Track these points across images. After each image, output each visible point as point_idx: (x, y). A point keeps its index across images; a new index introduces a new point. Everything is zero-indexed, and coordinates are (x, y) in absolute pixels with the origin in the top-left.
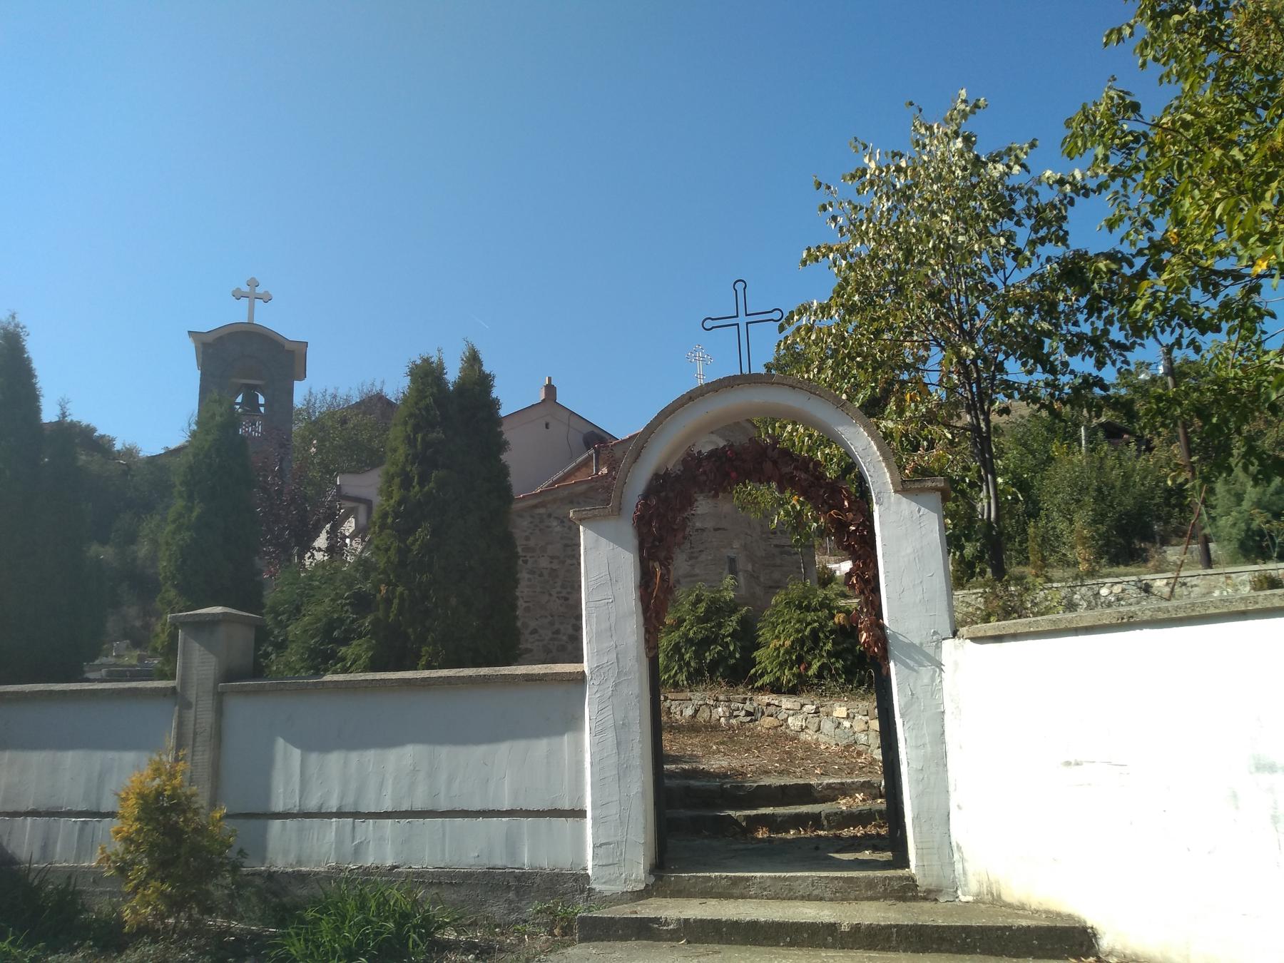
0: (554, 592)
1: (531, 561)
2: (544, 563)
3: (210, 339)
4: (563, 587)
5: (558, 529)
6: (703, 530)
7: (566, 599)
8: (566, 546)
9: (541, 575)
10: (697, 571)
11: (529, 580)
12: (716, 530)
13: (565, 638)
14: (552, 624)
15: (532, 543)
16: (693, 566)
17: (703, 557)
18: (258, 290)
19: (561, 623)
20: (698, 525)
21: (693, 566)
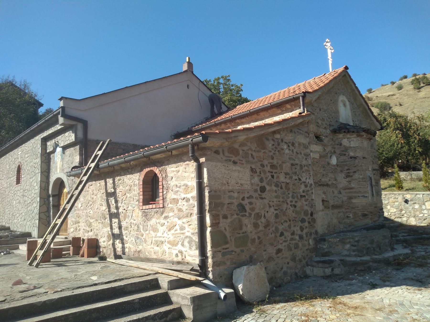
0: (288, 201)
1: (275, 176)
2: (282, 178)
4: (293, 197)
5: (287, 151)
6: (355, 158)
8: (292, 165)
9: (281, 188)
10: (353, 185)
11: (276, 192)
12: (364, 158)
13: (297, 238)
14: (290, 227)
15: (275, 162)
16: (349, 182)
17: (356, 176)
19: (295, 226)
20: (352, 154)
21: (349, 182)
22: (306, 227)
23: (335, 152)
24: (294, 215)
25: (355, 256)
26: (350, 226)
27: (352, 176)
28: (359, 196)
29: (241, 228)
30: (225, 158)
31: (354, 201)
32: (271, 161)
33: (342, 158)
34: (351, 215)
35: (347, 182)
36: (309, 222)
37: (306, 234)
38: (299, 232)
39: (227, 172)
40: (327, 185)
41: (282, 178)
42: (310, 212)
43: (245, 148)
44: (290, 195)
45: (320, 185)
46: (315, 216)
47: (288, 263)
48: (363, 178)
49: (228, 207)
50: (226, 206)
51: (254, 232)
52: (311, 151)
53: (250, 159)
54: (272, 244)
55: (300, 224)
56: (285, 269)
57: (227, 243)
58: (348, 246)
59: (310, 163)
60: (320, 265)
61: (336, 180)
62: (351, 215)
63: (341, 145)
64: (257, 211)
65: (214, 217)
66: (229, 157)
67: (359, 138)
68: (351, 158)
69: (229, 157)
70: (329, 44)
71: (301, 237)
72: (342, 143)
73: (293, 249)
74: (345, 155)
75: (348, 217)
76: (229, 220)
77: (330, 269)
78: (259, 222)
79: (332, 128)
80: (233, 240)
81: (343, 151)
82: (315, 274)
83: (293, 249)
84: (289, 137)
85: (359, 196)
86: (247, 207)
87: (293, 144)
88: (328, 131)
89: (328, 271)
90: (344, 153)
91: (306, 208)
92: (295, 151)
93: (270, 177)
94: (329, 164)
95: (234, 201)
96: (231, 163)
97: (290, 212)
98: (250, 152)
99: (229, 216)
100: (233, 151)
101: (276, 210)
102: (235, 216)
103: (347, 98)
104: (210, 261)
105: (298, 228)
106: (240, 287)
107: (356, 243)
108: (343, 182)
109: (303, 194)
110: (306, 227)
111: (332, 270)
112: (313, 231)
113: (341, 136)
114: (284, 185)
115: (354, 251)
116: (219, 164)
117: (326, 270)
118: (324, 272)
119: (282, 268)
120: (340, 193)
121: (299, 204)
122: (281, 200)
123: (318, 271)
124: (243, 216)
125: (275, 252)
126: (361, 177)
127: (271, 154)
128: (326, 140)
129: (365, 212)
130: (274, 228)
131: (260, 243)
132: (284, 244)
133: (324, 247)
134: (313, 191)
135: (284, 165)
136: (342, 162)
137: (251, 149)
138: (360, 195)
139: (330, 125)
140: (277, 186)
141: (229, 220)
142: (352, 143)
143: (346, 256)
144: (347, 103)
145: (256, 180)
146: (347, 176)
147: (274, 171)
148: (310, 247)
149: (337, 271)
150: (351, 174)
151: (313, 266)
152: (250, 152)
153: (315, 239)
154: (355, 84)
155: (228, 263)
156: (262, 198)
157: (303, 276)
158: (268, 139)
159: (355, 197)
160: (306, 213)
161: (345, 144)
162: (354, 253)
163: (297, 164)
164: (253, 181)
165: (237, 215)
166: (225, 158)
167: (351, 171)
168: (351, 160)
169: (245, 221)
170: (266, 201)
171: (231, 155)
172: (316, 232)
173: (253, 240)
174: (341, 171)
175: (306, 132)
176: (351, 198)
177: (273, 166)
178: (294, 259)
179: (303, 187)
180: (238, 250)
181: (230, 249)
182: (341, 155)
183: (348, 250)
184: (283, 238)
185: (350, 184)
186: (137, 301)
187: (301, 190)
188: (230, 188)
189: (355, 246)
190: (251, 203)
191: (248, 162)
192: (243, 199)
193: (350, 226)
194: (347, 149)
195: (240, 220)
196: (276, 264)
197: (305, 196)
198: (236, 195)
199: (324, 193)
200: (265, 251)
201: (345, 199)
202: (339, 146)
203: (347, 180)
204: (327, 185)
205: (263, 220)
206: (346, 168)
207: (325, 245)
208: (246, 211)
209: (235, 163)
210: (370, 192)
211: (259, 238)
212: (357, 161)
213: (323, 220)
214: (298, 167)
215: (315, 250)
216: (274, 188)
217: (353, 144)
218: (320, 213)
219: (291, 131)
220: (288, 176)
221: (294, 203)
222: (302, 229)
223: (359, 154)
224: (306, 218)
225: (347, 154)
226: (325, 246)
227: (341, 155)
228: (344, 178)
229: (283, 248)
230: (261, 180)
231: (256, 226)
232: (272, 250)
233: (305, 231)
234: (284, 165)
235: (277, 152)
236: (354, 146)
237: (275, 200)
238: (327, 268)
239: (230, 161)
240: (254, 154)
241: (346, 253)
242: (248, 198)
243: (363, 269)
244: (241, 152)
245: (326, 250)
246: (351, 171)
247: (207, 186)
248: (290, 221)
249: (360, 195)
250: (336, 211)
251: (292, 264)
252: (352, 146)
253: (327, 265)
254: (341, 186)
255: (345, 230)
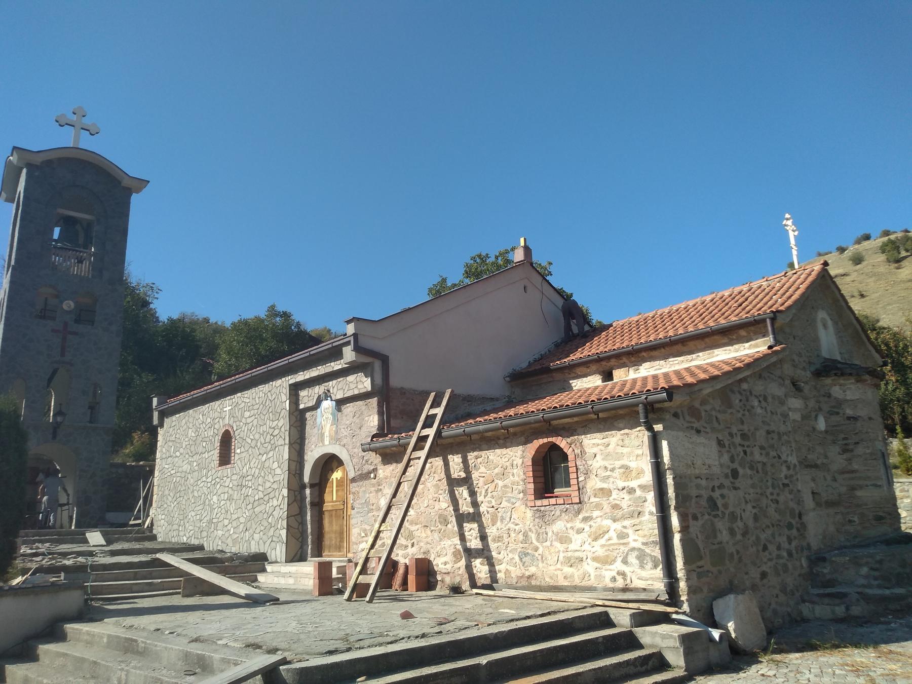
3: (38, 160)
5: (759, 411)
6: (855, 419)
7: (777, 502)
8: (768, 432)
9: (758, 472)
10: (855, 466)
13: (785, 554)
14: (773, 535)
15: (745, 428)
16: (849, 460)
17: (860, 450)
18: (86, 121)
19: (780, 535)
20: (849, 412)
21: (849, 460)
22: (795, 538)
23: (820, 409)
24: (778, 517)
25: (879, 587)
26: (856, 537)
27: (852, 451)
28: (867, 486)
29: (715, 537)
30: (686, 425)
31: (859, 493)
32: (741, 427)
33: (835, 419)
34: (856, 519)
35: (846, 460)
36: (798, 530)
37: (796, 548)
38: (786, 545)
39: (690, 446)
40: (816, 466)
41: (757, 457)
42: (797, 512)
43: (708, 408)
44: (769, 484)
45: (807, 466)
46: (805, 518)
47: (777, 596)
48: (871, 454)
49: (697, 503)
50: (694, 500)
51: (731, 543)
52: (789, 409)
53: (716, 425)
54: (754, 564)
55: (786, 531)
56: (773, 606)
57: (701, 558)
58: (865, 570)
59: (790, 429)
60: (826, 600)
61: (826, 457)
62: (856, 519)
63: (829, 396)
64: (731, 509)
65: (683, 518)
66: (691, 422)
67: (859, 385)
68: (849, 418)
69: (691, 422)
70: (789, 222)
71: (790, 554)
72: (832, 392)
73: (781, 573)
74: (838, 413)
75: (850, 521)
76: (700, 522)
77: (843, 608)
78: (734, 526)
79: (813, 368)
80: (708, 553)
81: (834, 407)
82: (817, 615)
83: (781, 573)
84: (759, 387)
85: (867, 486)
86: (720, 502)
87: (765, 399)
88: (808, 374)
89: (840, 610)
90: (836, 410)
91: (792, 505)
92: (769, 409)
93: (742, 454)
94: (814, 429)
95: (703, 492)
96: (694, 432)
97: (771, 511)
98: (714, 413)
99: (699, 516)
100: (695, 413)
101: (754, 507)
102: (707, 517)
103: (829, 315)
104: (683, 585)
105: (785, 539)
106: (731, 626)
107: (877, 566)
108: (838, 461)
109: (786, 481)
110: (795, 538)
111: (847, 609)
112: (805, 544)
113: (828, 381)
114: (760, 466)
115: (876, 579)
116: (680, 434)
117: (837, 608)
118: (833, 612)
119: (770, 604)
120: (835, 480)
121: (781, 499)
122: (759, 491)
123: (822, 610)
124: (716, 516)
125: (759, 576)
126: (868, 451)
127: (740, 415)
128: (806, 389)
129: (881, 514)
130: (754, 538)
131: (740, 560)
132: (770, 564)
133: (825, 571)
134: (799, 476)
135: (758, 433)
136: (833, 426)
137: (714, 409)
138: (869, 483)
139: (810, 363)
140: (752, 468)
141: (700, 522)
142: (848, 392)
143: (864, 586)
144: (830, 323)
145: (726, 458)
146: (845, 451)
147: (746, 443)
148: (803, 571)
149: (856, 610)
150: (851, 447)
151: (813, 602)
152: (714, 413)
153: (808, 558)
154: (839, 290)
155: (705, 590)
156: (735, 488)
157: (799, 619)
158: (733, 392)
159: (861, 487)
160: (792, 512)
161: (837, 395)
162: (876, 583)
163: (773, 432)
164: (722, 461)
165: (709, 514)
166: (686, 425)
167: (850, 441)
168: (848, 422)
169: (720, 525)
170: (741, 493)
171: (693, 420)
172: (809, 547)
173: (732, 555)
174: (834, 442)
175: (780, 377)
176: (853, 489)
177: (744, 436)
178: (784, 590)
179: (784, 468)
180: (715, 570)
181: (705, 568)
182: (831, 414)
183: (866, 577)
184: (766, 553)
185: (850, 464)
186: (600, 640)
187: (782, 476)
188: (697, 471)
189: (876, 570)
190: (723, 496)
191: (714, 430)
192: (713, 490)
193: (856, 537)
194: (840, 403)
195: (713, 524)
196: (762, 597)
197: (788, 485)
198: (703, 483)
199: (813, 480)
200: (747, 573)
201: (843, 490)
202: (826, 399)
203: (845, 456)
204: (816, 466)
205: (740, 524)
206: (843, 436)
207: (825, 568)
208: (718, 509)
209: (698, 431)
210: (884, 477)
211: (738, 552)
212: (859, 424)
213: (818, 526)
214: (776, 436)
215: (811, 577)
216: (749, 472)
217: (849, 396)
218: (812, 514)
219: (760, 377)
220: (764, 452)
221: (774, 497)
222: (790, 541)
223: (862, 412)
224: (794, 522)
225: (841, 411)
226: (826, 570)
227: (831, 413)
228: (839, 454)
229: (768, 570)
230: (732, 460)
231: (732, 532)
232: (755, 573)
233: (794, 544)
234: (758, 433)
235: (747, 413)
236: (853, 398)
237: (751, 491)
238: (838, 605)
239: (692, 428)
240: (719, 416)
241: (862, 581)
242: (719, 487)
243: (899, 608)
244: (703, 414)
245: (828, 577)
246: (850, 441)
247: (669, 469)
248: (773, 526)
249: (869, 483)
250: (831, 511)
251: (782, 598)
252: (848, 398)
253: (837, 601)
254: (835, 467)
255: (848, 544)
